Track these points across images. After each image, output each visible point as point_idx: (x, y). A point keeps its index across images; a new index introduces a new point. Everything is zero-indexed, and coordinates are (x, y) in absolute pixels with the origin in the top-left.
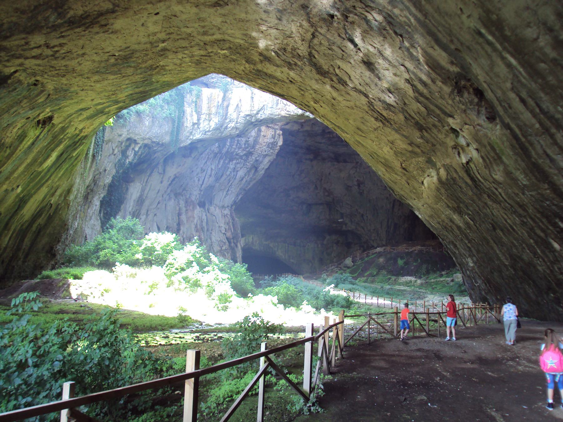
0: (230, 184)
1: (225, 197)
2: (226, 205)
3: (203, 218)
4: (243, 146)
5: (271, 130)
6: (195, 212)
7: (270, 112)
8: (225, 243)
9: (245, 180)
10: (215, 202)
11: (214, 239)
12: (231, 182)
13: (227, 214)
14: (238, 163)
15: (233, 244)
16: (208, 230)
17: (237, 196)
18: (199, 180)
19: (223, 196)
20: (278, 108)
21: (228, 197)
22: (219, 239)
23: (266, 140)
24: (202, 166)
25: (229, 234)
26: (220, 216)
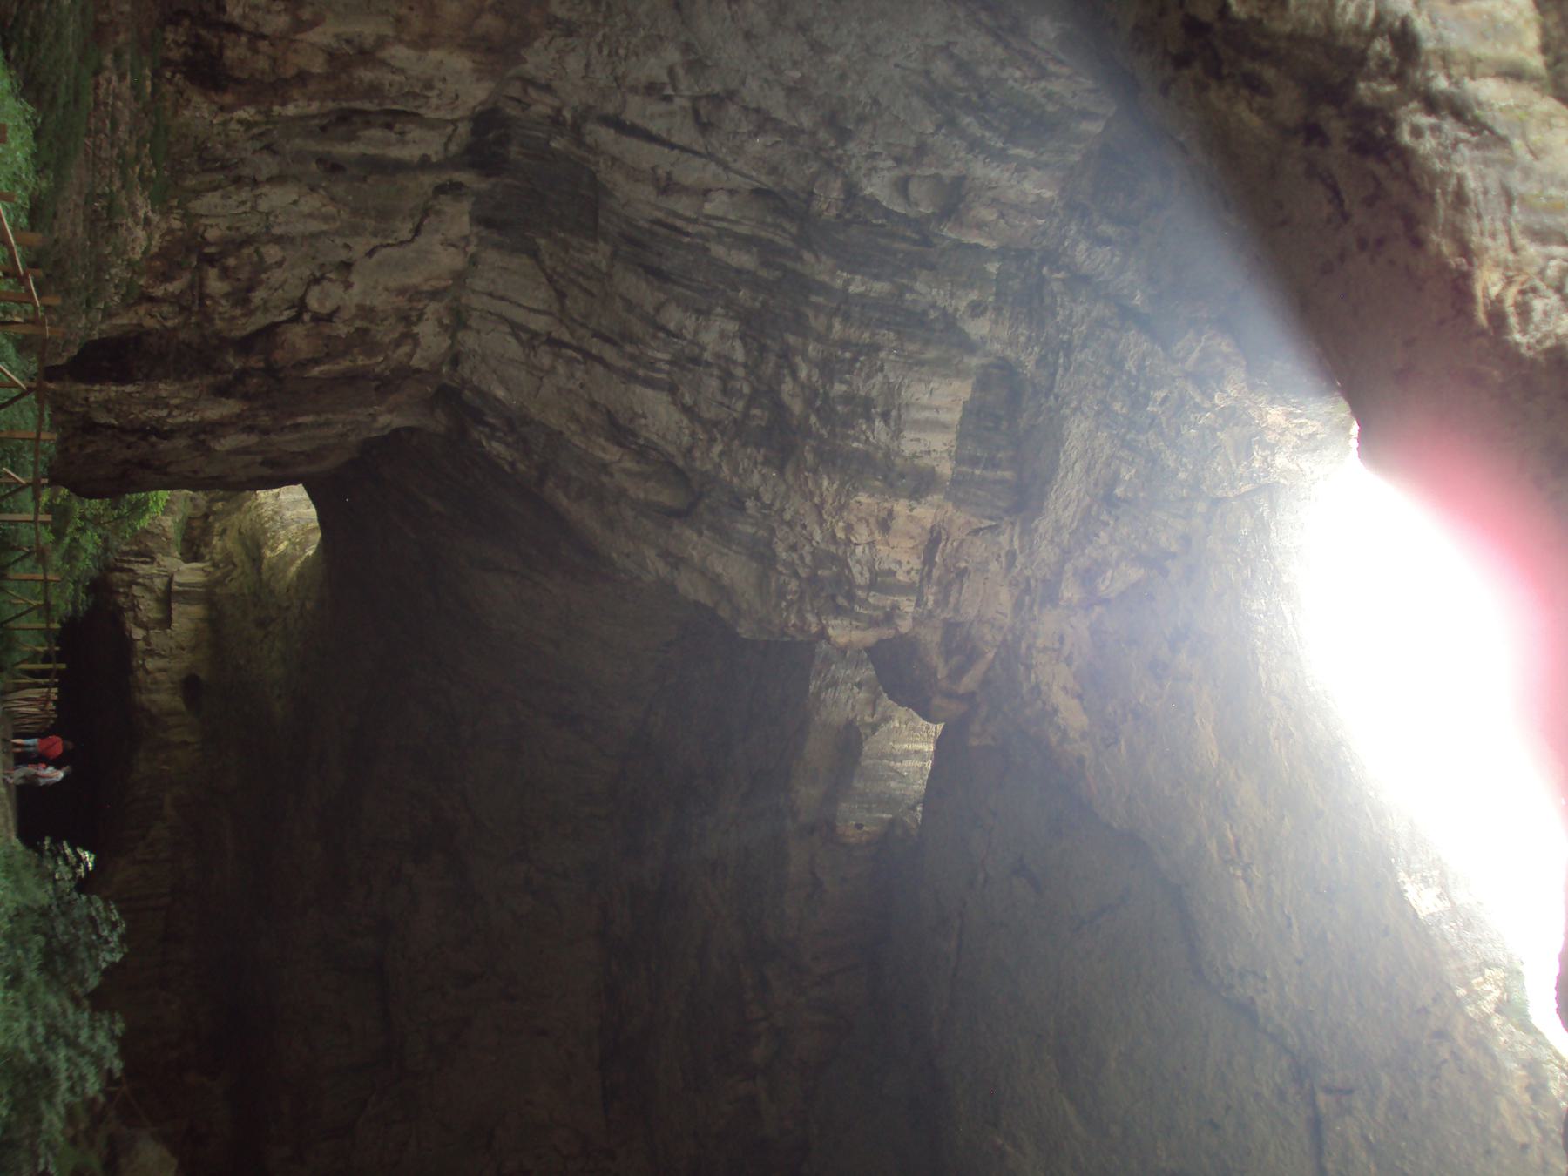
0: (596, 347)
1: (516, 328)
2: (469, 340)
3: (415, 133)
4: (839, 388)
5: (916, 564)
6: (460, 63)
7: (1472, 184)
8: (241, 297)
9: (611, 454)
10: (491, 256)
11: (276, 198)
12: (609, 353)
13: (415, 339)
14: (727, 377)
15: (234, 362)
16: (334, 167)
17: (515, 424)
18: (652, 89)
19: (518, 315)
20: (1522, 241)
21: (513, 348)
22: (273, 253)
23: (862, 534)
24: (752, 91)
25: (298, 339)
26: (415, 279)
